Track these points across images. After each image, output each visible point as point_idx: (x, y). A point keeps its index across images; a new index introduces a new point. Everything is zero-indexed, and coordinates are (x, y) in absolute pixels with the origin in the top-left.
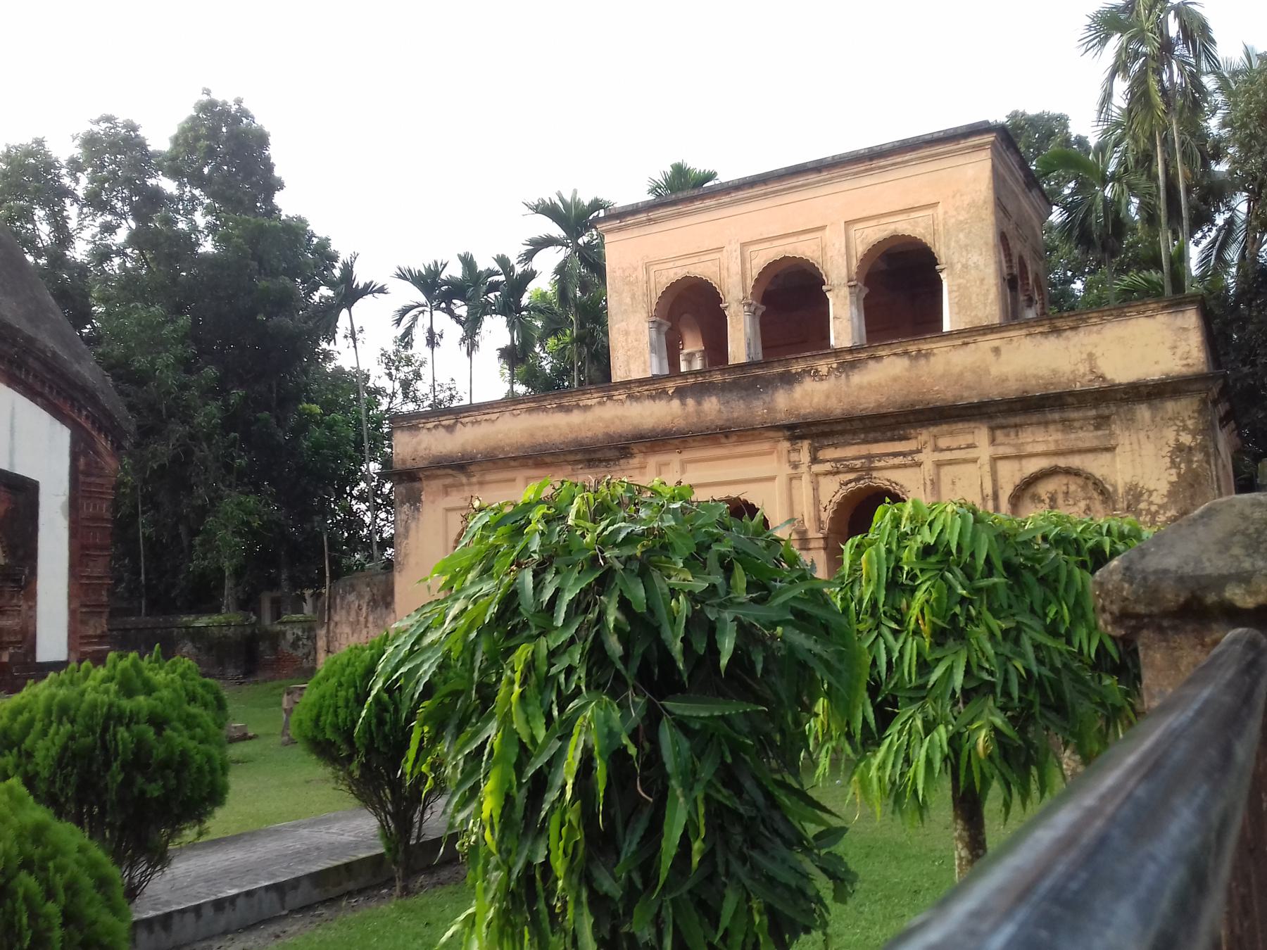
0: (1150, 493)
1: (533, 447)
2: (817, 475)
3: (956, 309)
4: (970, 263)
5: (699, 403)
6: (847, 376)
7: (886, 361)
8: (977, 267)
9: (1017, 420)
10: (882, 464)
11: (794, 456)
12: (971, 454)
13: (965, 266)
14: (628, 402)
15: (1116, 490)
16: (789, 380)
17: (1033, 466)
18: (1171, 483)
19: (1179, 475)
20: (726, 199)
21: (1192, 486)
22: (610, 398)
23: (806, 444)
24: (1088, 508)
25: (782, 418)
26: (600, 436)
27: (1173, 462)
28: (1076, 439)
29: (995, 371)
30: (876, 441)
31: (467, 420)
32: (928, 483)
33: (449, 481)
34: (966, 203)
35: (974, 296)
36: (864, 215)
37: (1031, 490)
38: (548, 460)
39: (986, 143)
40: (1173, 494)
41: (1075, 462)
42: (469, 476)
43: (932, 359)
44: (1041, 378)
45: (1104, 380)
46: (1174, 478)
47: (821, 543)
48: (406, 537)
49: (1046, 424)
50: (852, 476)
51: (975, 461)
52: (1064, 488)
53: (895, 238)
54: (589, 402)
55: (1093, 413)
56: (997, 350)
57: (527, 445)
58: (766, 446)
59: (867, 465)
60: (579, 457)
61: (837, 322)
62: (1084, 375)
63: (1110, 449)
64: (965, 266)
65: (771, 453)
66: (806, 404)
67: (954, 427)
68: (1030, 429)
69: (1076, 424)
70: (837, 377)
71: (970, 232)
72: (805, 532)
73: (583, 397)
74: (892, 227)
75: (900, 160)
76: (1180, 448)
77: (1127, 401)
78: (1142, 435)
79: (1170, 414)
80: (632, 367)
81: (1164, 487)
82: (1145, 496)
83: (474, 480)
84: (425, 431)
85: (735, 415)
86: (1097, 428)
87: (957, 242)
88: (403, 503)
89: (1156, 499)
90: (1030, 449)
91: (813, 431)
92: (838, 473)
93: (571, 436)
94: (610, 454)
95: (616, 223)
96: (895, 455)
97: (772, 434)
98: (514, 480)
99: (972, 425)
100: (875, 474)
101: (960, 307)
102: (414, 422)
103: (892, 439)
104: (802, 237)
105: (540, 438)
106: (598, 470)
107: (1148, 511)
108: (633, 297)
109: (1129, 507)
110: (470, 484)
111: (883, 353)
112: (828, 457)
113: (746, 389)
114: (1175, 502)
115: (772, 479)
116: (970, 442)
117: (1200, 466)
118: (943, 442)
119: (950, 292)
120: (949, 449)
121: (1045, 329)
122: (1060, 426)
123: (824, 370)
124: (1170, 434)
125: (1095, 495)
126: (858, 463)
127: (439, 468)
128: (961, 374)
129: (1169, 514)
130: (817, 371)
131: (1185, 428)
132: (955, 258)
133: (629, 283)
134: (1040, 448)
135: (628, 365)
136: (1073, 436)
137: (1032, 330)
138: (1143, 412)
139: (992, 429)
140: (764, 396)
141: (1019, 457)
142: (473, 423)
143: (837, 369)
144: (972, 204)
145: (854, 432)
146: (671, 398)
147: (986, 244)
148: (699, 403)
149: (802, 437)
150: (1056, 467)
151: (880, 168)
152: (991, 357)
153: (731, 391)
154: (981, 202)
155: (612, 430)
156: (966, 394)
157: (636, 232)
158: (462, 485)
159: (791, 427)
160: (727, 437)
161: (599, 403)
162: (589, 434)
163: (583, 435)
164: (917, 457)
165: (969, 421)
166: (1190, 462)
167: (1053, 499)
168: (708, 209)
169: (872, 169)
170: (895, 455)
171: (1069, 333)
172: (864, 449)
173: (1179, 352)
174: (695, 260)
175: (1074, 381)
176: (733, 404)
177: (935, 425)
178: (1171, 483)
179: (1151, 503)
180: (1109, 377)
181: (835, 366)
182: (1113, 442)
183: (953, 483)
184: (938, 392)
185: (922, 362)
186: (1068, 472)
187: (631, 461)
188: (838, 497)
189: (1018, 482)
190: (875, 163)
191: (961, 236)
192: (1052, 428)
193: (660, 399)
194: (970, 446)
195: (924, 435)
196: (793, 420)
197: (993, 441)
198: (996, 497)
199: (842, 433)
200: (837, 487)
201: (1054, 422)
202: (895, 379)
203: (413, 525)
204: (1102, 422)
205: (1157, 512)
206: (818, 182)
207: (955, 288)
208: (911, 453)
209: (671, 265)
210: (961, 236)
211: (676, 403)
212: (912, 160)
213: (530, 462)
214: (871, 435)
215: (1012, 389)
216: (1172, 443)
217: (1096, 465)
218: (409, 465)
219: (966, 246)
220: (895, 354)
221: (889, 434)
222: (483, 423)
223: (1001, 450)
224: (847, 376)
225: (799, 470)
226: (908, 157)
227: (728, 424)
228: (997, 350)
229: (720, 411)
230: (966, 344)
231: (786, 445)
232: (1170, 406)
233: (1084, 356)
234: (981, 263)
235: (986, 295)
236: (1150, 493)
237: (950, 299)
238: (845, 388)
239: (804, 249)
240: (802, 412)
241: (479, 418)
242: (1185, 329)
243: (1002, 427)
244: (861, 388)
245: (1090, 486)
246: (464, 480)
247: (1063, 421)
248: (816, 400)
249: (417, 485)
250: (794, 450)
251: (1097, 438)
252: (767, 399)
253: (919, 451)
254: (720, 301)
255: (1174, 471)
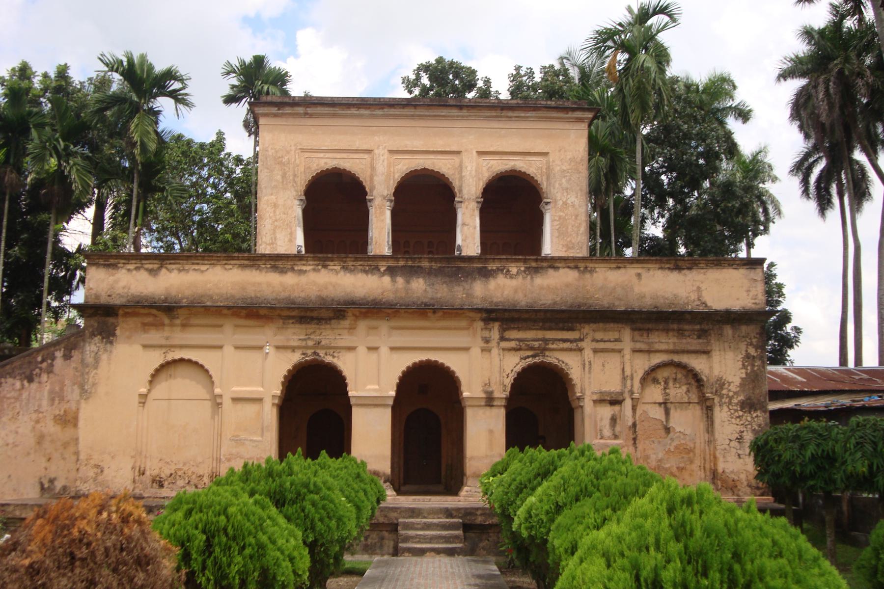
0: (730, 383)
1: (244, 299)
2: (504, 349)
3: (556, 234)
4: (569, 202)
5: (408, 282)
6: (532, 278)
7: (562, 271)
8: (573, 206)
9: (650, 326)
10: (554, 346)
11: (486, 334)
12: (618, 346)
13: (565, 203)
14: (342, 273)
15: (708, 380)
16: (486, 274)
17: (657, 359)
18: (742, 378)
19: (746, 373)
20: (380, 112)
21: (754, 381)
22: (325, 266)
23: (496, 325)
24: (688, 391)
25: (478, 303)
26: (313, 298)
27: (743, 365)
28: (688, 343)
29: (637, 289)
30: (551, 329)
31: (173, 266)
32: (587, 363)
33: (149, 320)
34: (568, 157)
35: (570, 227)
36: (492, 149)
37: (653, 375)
38: (262, 312)
39: (586, 118)
40: (742, 385)
41: (684, 359)
42: (172, 318)
43: (595, 275)
44: (667, 299)
45: (706, 306)
46: (744, 376)
47: (503, 403)
48: (96, 368)
49: (667, 331)
50: (530, 353)
51: (620, 351)
52: (674, 376)
53: (513, 171)
54: (304, 268)
55: (698, 327)
56: (639, 275)
57: (237, 296)
58: (464, 323)
59: (543, 346)
60: (294, 313)
61: (466, 228)
62: (694, 301)
63: (707, 353)
64: (565, 203)
65: (467, 329)
66: (499, 295)
67: (608, 326)
68: (656, 333)
69: (687, 333)
70: (524, 278)
71: (570, 179)
72: (492, 392)
73: (299, 263)
74: (512, 163)
75: (523, 115)
76: (748, 356)
77: (719, 322)
78: (726, 345)
79: (743, 334)
80: (278, 236)
81: (737, 381)
82: (726, 386)
83: (178, 322)
84: (124, 271)
85: (439, 295)
86: (699, 337)
87: (560, 184)
88: (93, 335)
89: (733, 388)
90: (657, 347)
91: (504, 318)
92: (520, 349)
93: (284, 295)
94: (325, 314)
95: (274, 110)
96: (565, 341)
97: (472, 314)
98: (221, 326)
99: (620, 326)
100: (547, 353)
101: (561, 232)
102: (112, 261)
103: (562, 329)
104: (439, 157)
105: (251, 292)
106: (309, 326)
107: (728, 396)
108: (284, 176)
109: (716, 391)
110: (172, 325)
111: (559, 265)
112: (512, 337)
113: (449, 276)
114: (743, 391)
115: (467, 349)
116: (617, 337)
117: (759, 369)
118: (599, 335)
119: (553, 221)
120: (602, 341)
121: (671, 266)
122: (676, 334)
123: (514, 270)
124: (743, 346)
125: (693, 382)
126: (536, 344)
127: (144, 307)
128: (615, 288)
129: (739, 398)
130: (508, 271)
131: (751, 344)
132: (559, 196)
133: (281, 163)
134: (663, 347)
135: (274, 233)
136: (684, 341)
137: (663, 265)
138: (728, 331)
139: (633, 330)
140: (464, 284)
141: (649, 352)
142: (180, 271)
143: (524, 271)
144: (572, 160)
145: (535, 321)
146: (383, 274)
147: (581, 190)
148: (408, 282)
149: (495, 320)
150: (672, 361)
151: (507, 117)
152: (635, 279)
153: (436, 276)
154: (578, 160)
155: (325, 293)
156: (617, 303)
157: (291, 121)
158: (163, 325)
159: (489, 311)
160: (434, 312)
161: (314, 270)
162: (303, 295)
163: (296, 294)
164: (580, 344)
165: (618, 323)
166: (753, 366)
167: (666, 382)
168: (361, 116)
169: (501, 117)
170: (565, 341)
171: (685, 271)
172: (540, 334)
173: (751, 294)
174: (344, 155)
175: (688, 304)
176: (437, 287)
177: (595, 322)
178: (742, 378)
179: (729, 390)
180: (709, 305)
181: (522, 269)
182: (709, 348)
183: (603, 365)
184: (598, 299)
185: (588, 276)
186: (680, 366)
187: (342, 322)
188: (519, 368)
189: (647, 369)
190: (504, 113)
191: (564, 181)
192: (671, 334)
193: (373, 274)
194: (616, 340)
195: (587, 329)
196: (487, 305)
197: (633, 340)
198: (632, 379)
199: (525, 320)
200: (517, 360)
201: (673, 330)
202: (568, 285)
203: (104, 357)
204: (703, 334)
205: (733, 396)
206: (458, 116)
207: (557, 218)
208: (575, 341)
209: (322, 155)
210: (564, 181)
211: (387, 279)
212: (532, 117)
213: (244, 312)
214: (547, 325)
215: (647, 304)
216: (744, 353)
217: (698, 364)
218: (104, 300)
219: (567, 189)
220: (568, 267)
221: (561, 325)
222: (191, 272)
223: (639, 346)
224: (532, 278)
225: (490, 345)
226: (530, 114)
227: (432, 302)
228: (639, 275)
229: (425, 290)
230: (619, 268)
231: (480, 324)
232: (744, 329)
233: (695, 288)
234: (577, 203)
235: (579, 227)
236: (730, 383)
237: (552, 226)
238: (529, 286)
239: (442, 165)
240: (495, 300)
241: (187, 267)
242: (755, 280)
243: (640, 330)
244: (542, 288)
245: (690, 376)
246: (167, 321)
247: (679, 330)
248: (506, 293)
249: (111, 320)
250: (486, 329)
251: (699, 344)
252: (467, 287)
253: (581, 340)
254: (366, 194)
255: (743, 371)
